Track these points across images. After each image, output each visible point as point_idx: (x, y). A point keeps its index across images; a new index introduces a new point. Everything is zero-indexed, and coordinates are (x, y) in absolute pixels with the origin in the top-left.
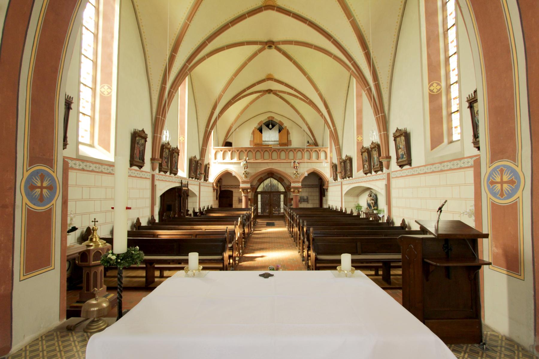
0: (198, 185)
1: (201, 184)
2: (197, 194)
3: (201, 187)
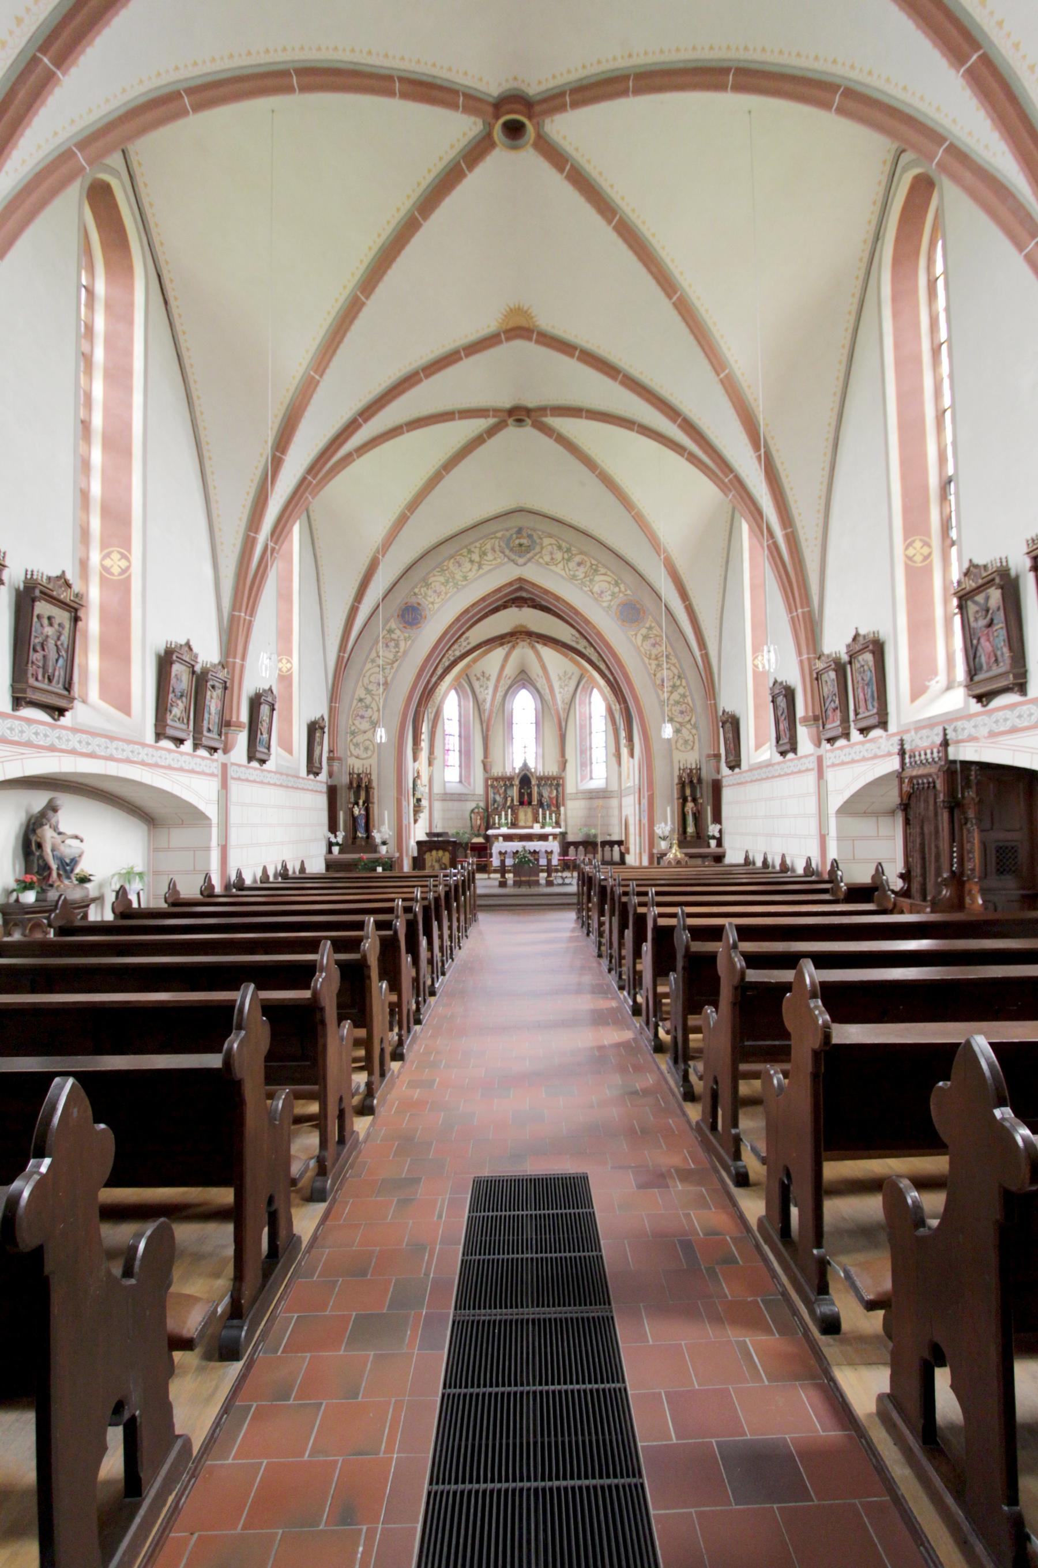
0: (212, 775)
1: (232, 772)
2: (211, 811)
3: (234, 786)
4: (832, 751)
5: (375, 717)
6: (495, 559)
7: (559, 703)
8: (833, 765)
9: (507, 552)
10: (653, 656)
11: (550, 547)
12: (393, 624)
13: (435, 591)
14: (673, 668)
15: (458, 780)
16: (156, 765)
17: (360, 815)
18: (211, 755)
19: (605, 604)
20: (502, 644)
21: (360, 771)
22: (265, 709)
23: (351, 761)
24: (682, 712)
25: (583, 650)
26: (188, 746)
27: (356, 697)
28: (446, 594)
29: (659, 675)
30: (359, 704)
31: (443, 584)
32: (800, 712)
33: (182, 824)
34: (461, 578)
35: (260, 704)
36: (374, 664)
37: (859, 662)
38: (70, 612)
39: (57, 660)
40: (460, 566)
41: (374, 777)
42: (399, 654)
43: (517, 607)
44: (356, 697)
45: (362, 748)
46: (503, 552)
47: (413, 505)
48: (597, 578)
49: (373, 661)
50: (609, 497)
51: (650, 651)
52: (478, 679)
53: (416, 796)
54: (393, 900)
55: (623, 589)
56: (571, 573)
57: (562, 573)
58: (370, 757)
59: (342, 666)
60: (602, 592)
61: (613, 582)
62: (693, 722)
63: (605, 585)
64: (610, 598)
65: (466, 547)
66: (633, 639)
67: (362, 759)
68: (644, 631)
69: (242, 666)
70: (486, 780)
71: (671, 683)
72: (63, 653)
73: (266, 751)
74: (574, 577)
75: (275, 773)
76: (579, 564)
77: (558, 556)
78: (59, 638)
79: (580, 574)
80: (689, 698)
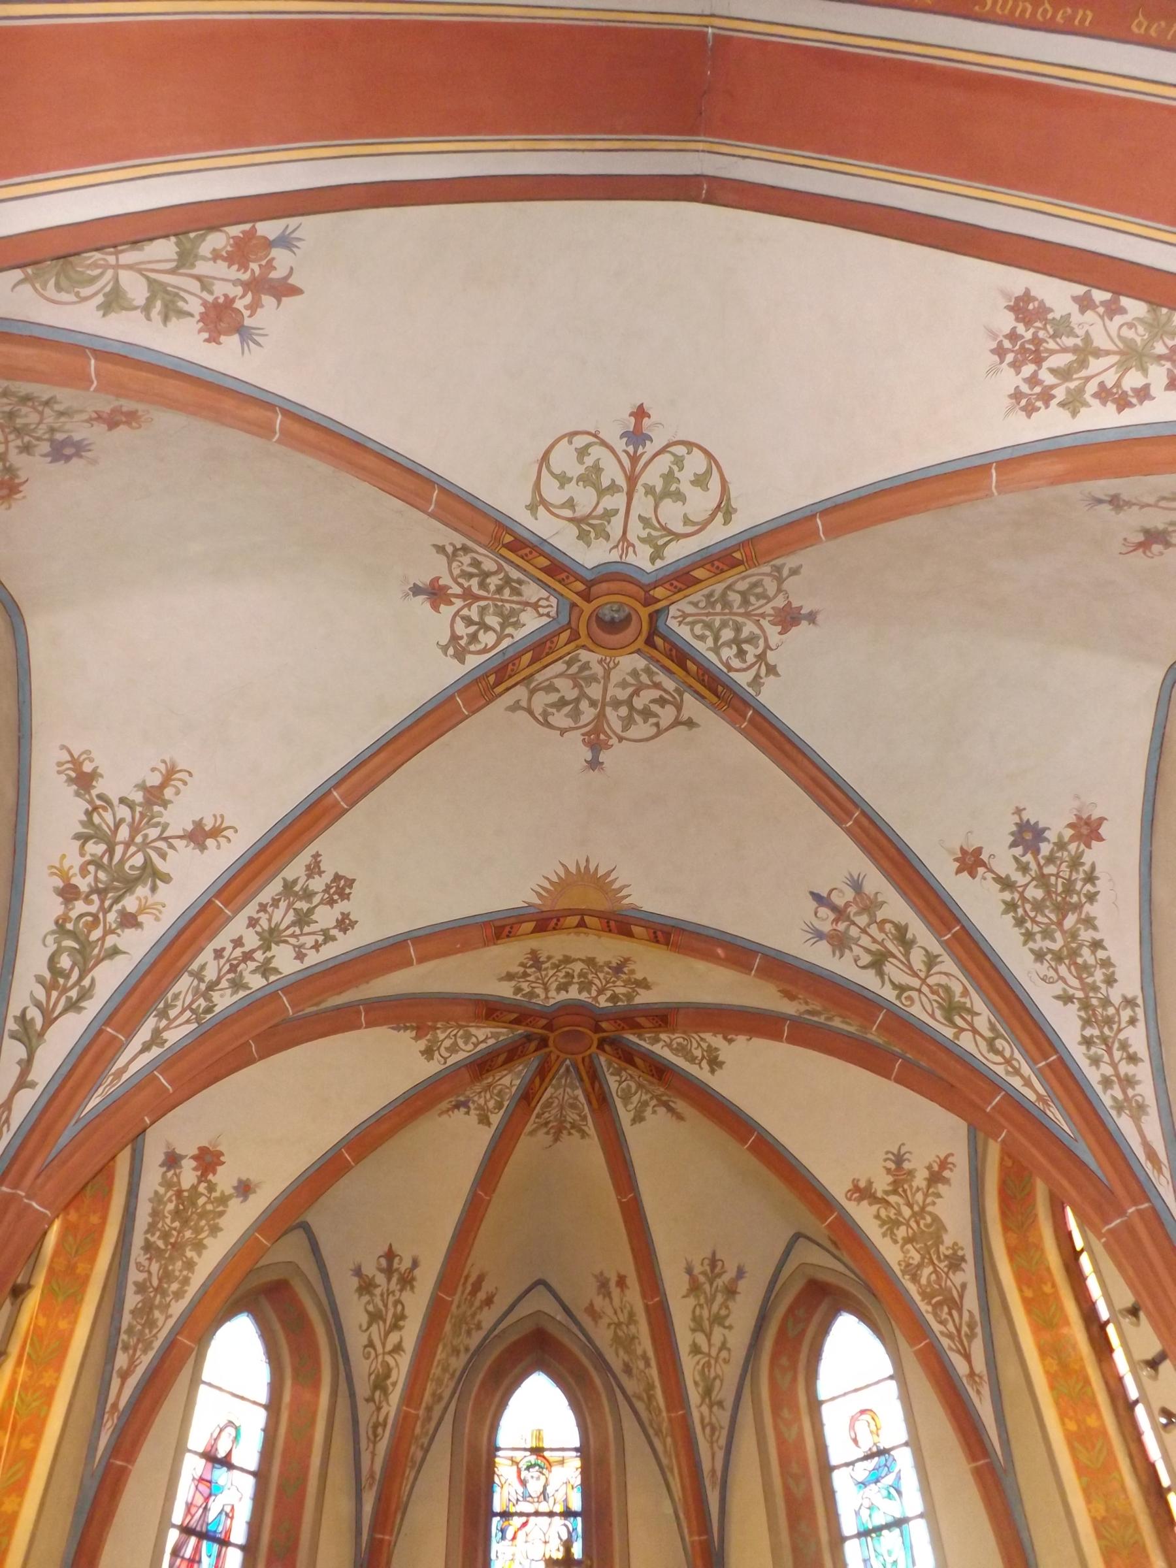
7: (694, 1396)
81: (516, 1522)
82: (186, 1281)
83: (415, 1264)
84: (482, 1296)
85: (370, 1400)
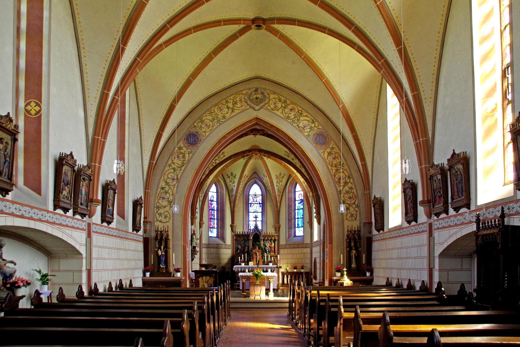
0: (83, 229)
1: (93, 228)
3: (94, 236)
4: (437, 220)
5: (171, 198)
6: (241, 106)
7: (276, 192)
8: (438, 228)
9: (249, 102)
10: (334, 165)
11: (274, 100)
12: (181, 144)
13: (206, 125)
14: (345, 172)
15: (216, 236)
16: (54, 223)
17: (162, 255)
18: (83, 218)
19: (306, 134)
20: (243, 157)
21: (162, 230)
22: (111, 192)
23: (157, 224)
24: (350, 198)
25: (292, 161)
26: (70, 213)
27: (160, 186)
28: (213, 127)
29: (337, 176)
30: (162, 191)
31: (211, 121)
32: (420, 198)
33: (66, 257)
34: (222, 118)
35: (108, 189)
36: (171, 167)
37: (454, 169)
38: (12, 136)
39: (5, 163)
40: (221, 110)
41: (170, 233)
42: (185, 162)
43: (253, 134)
44: (160, 186)
45: (163, 217)
46: (246, 102)
47: (194, 75)
48: (302, 118)
49: (170, 166)
50: (310, 72)
51: (332, 161)
52: (229, 177)
53: (193, 245)
54: (192, 303)
55: (317, 125)
56: (287, 115)
57: (282, 115)
58: (166, 222)
59: (152, 168)
60: (305, 127)
61: (311, 121)
62: (356, 204)
63: (306, 123)
64: (309, 130)
65: (225, 99)
66: (322, 155)
67: (163, 223)
68: (329, 150)
69: (99, 168)
70: (233, 237)
71: (344, 181)
72: (8, 159)
73: (111, 217)
74: (288, 117)
75: (116, 229)
76: (291, 110)
77: (279, 105)
78: (5, 151)
79: (292, 115)
80: (354, 190)
81: (252, 205)
82: (206, 185)
83: (236, 175)
84: (246, 176)
85: (231, 192)
